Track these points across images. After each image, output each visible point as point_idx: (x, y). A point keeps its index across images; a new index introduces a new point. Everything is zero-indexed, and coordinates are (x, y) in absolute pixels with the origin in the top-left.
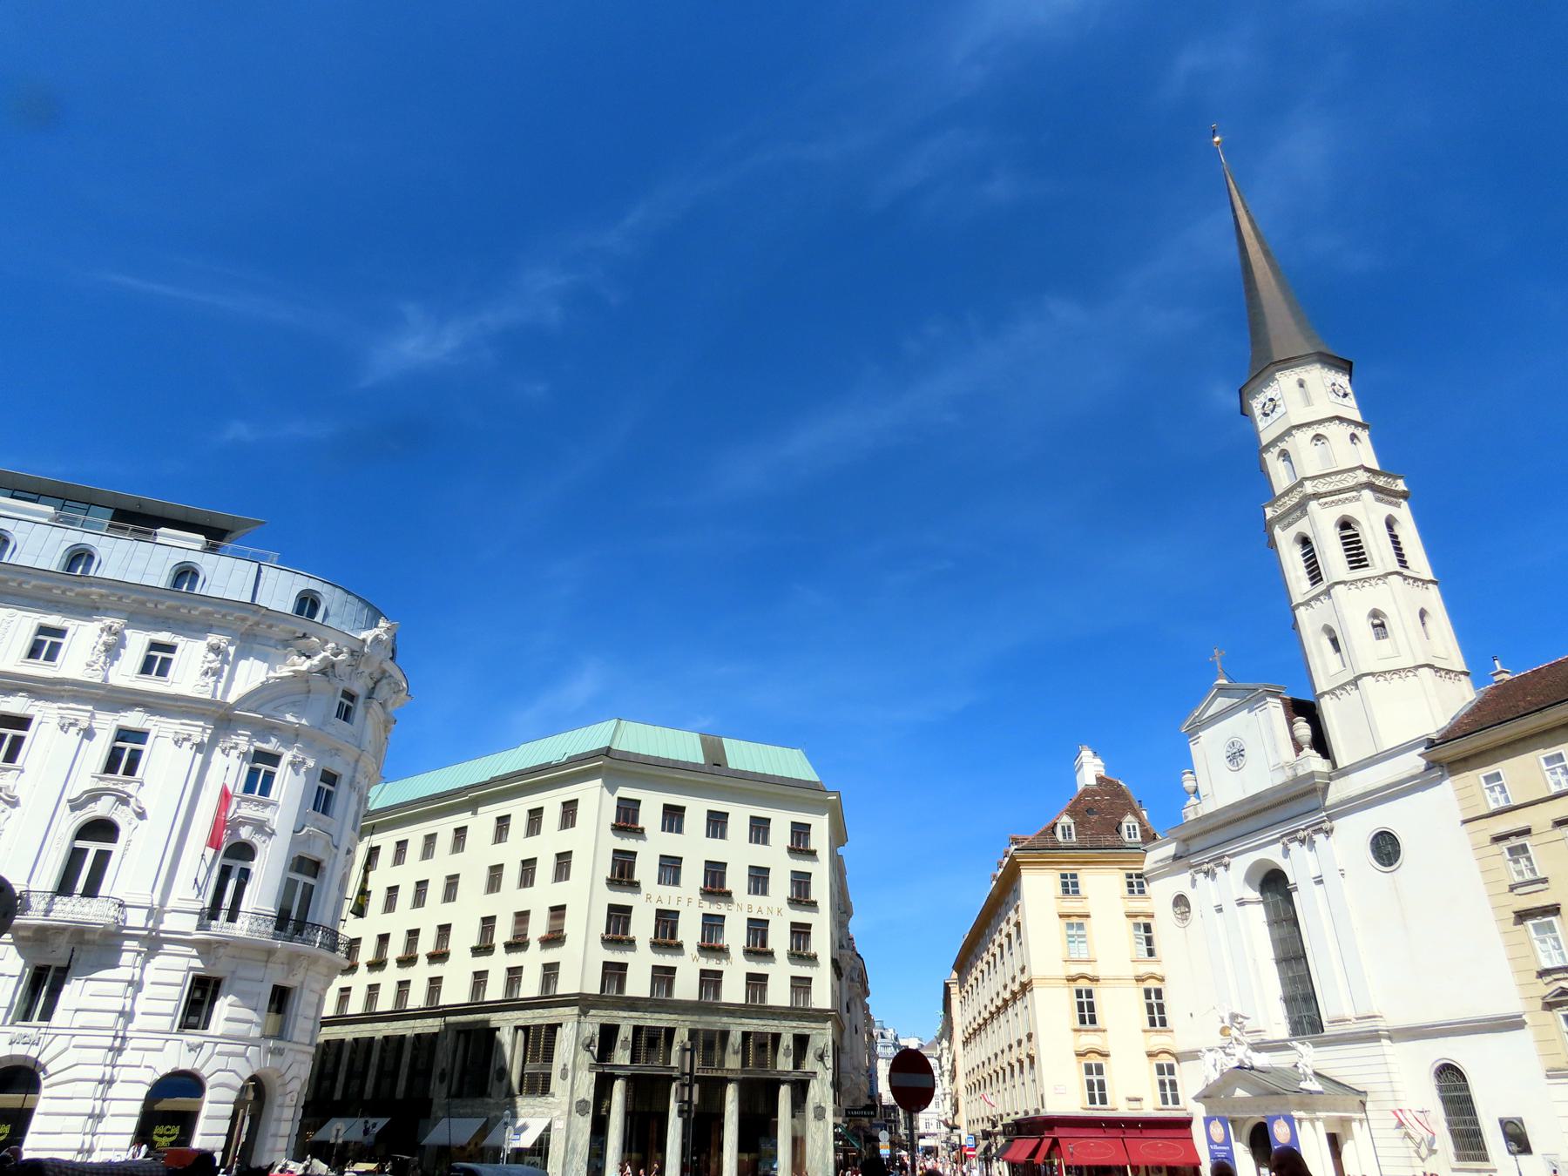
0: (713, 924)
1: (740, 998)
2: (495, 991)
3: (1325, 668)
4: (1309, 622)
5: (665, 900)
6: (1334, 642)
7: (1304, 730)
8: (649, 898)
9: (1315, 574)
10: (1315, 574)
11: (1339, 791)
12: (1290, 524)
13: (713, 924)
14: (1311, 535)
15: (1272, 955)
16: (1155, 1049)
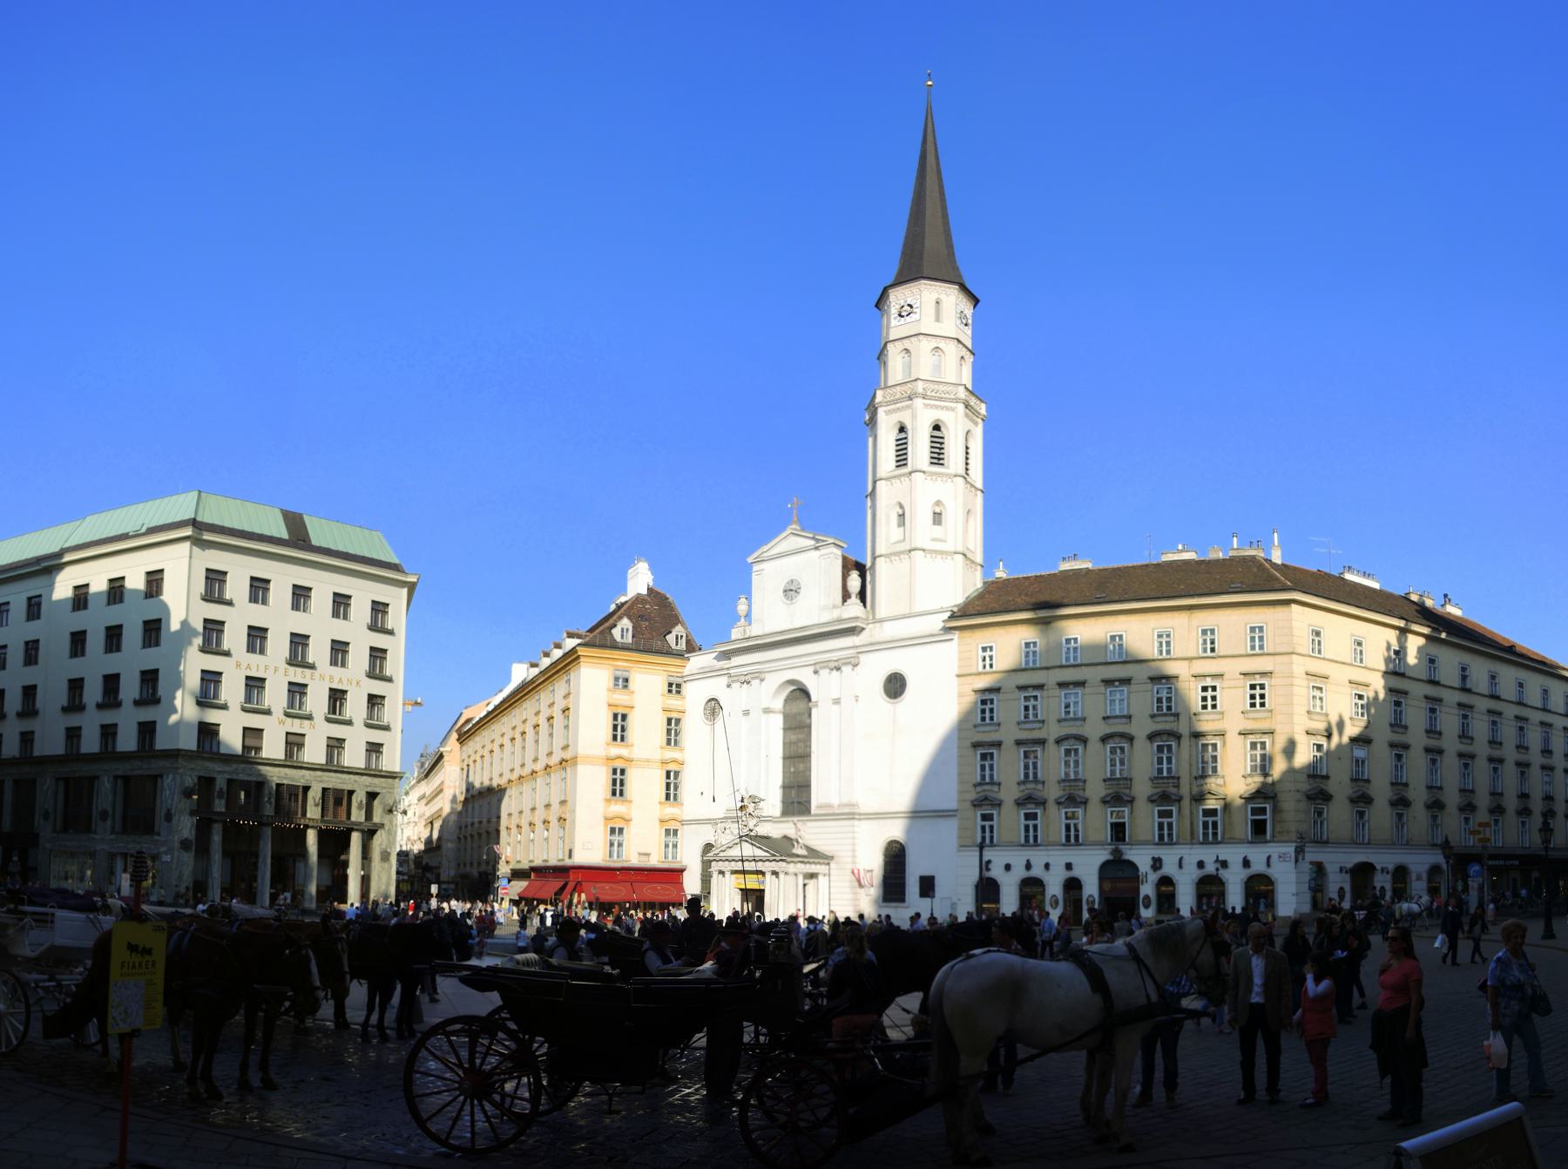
0: (297, 690)
1: (321, 758)
2: (90, 743)
3: (887, 534)
4: (887, 495)
5: (254, 668)
6: (902, 516)
7: (854, 581)
8: (238, 665)
9: (902, 459)
10: (902, 459)
11: (872, 633)
12: (894, 411)
13: (297, 690)
14: (909, 426)
15: (780, 782)
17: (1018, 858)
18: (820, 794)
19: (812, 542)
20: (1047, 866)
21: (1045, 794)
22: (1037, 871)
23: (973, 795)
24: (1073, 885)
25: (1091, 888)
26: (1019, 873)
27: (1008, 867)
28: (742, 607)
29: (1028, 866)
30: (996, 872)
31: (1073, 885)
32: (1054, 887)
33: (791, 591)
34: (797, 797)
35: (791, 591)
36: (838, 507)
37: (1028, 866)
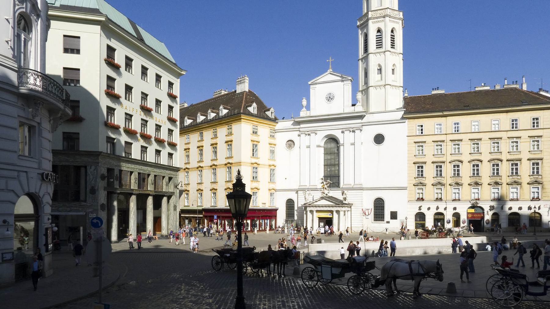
16: (253, 187)
17: (433, 206)
18: (346, 179)
19: (339, 78)
20: (445, 209)
21: (444, 182)
22: (441, 210)
23: (414, 182)
24: (457, 216)
25: (464, 217)
26: (433, 211)
27: (429, 209)
28: (304, 102)
29: (438, 208)
30: (424, 210)
31: (457, 216)
32: (449, 216)
33: (330, 98)
34: (332, 178)
35: (330, 98)
36: (350, 63)
37: (438, 208)
